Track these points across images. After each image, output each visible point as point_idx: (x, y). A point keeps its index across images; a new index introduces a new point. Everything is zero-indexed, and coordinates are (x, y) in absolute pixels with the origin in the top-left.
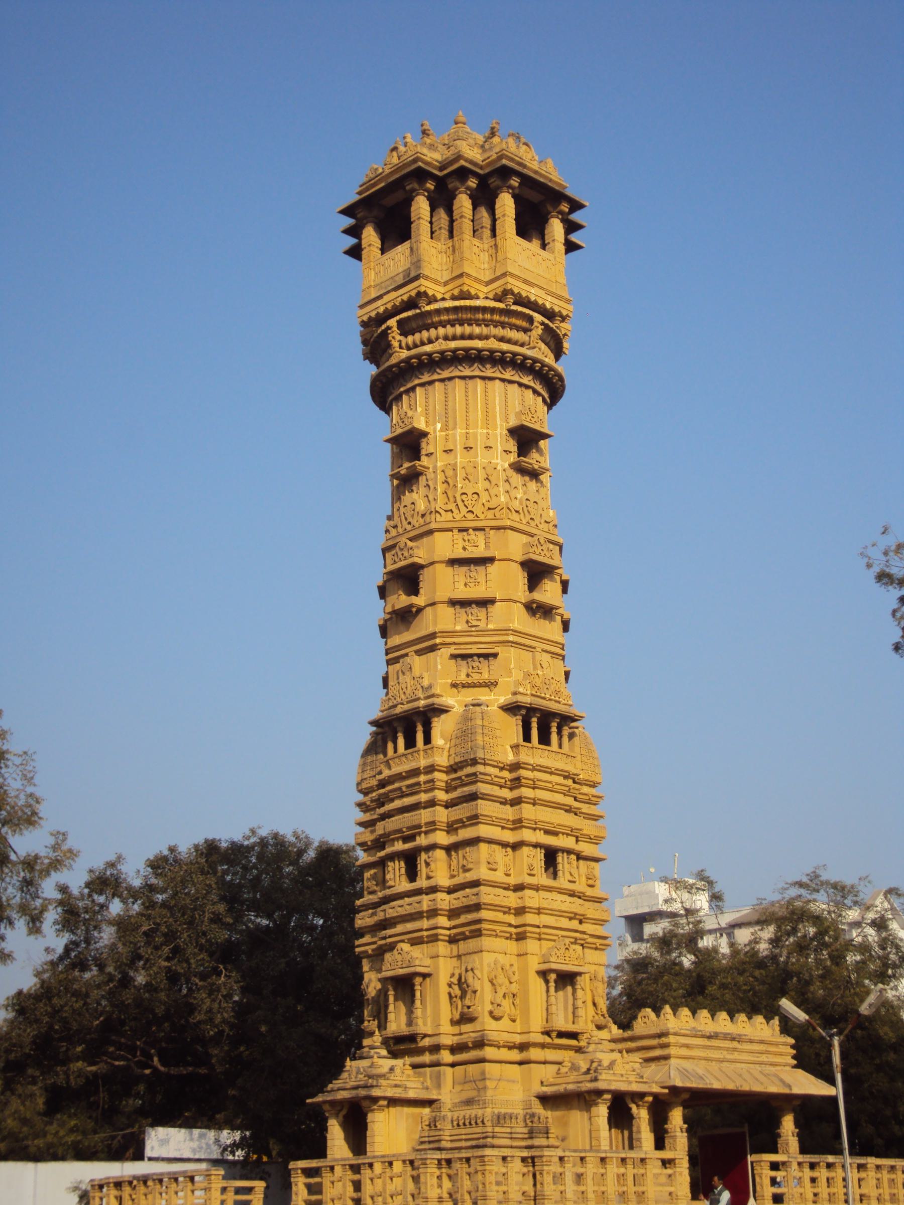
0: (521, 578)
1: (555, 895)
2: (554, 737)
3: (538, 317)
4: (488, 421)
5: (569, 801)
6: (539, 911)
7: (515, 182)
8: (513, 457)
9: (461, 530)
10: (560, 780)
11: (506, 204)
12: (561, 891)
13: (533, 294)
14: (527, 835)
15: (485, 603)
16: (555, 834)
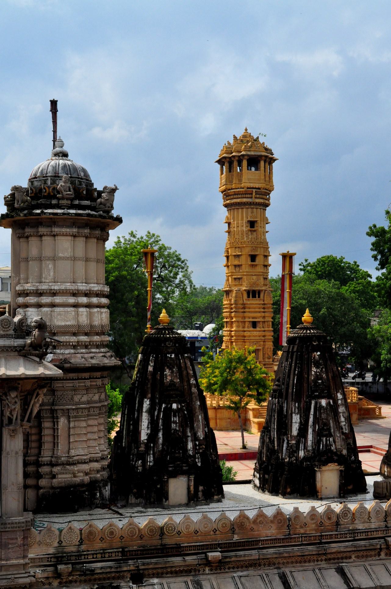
0: (249, 259)
1: (255, 333)
2: (257, 296)
3: (254, 190)
4: (242, 219)
5: (263, 310)
6: (250, 336)
7: (246, 157)
8: (249, 228)
9: (236, 248)
10: (258, 306)
11: (245, 163)
12: (256, 331)
13: (252, 185)
14: (247, 320)
15: (239, 266)
16: (256, 318)
